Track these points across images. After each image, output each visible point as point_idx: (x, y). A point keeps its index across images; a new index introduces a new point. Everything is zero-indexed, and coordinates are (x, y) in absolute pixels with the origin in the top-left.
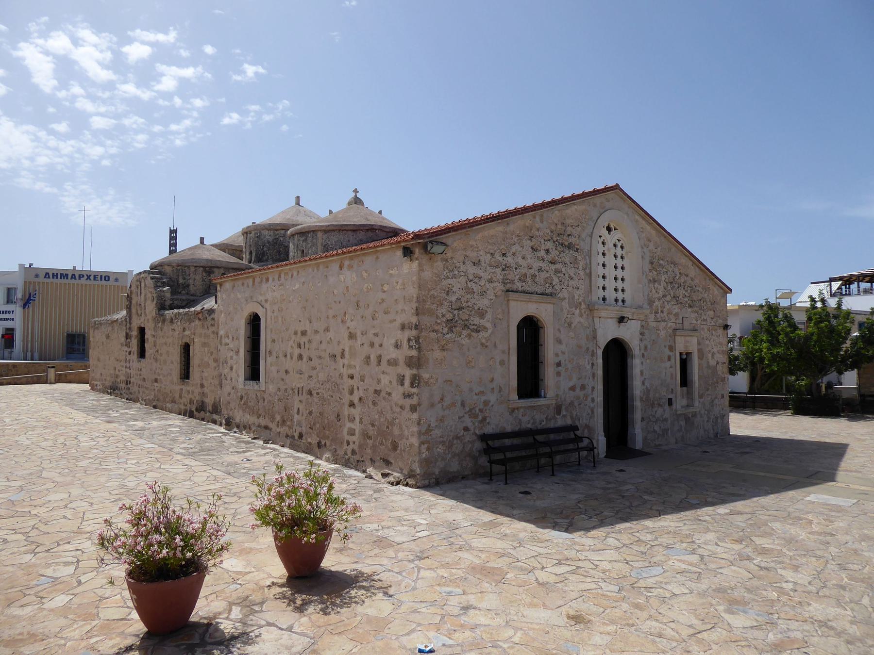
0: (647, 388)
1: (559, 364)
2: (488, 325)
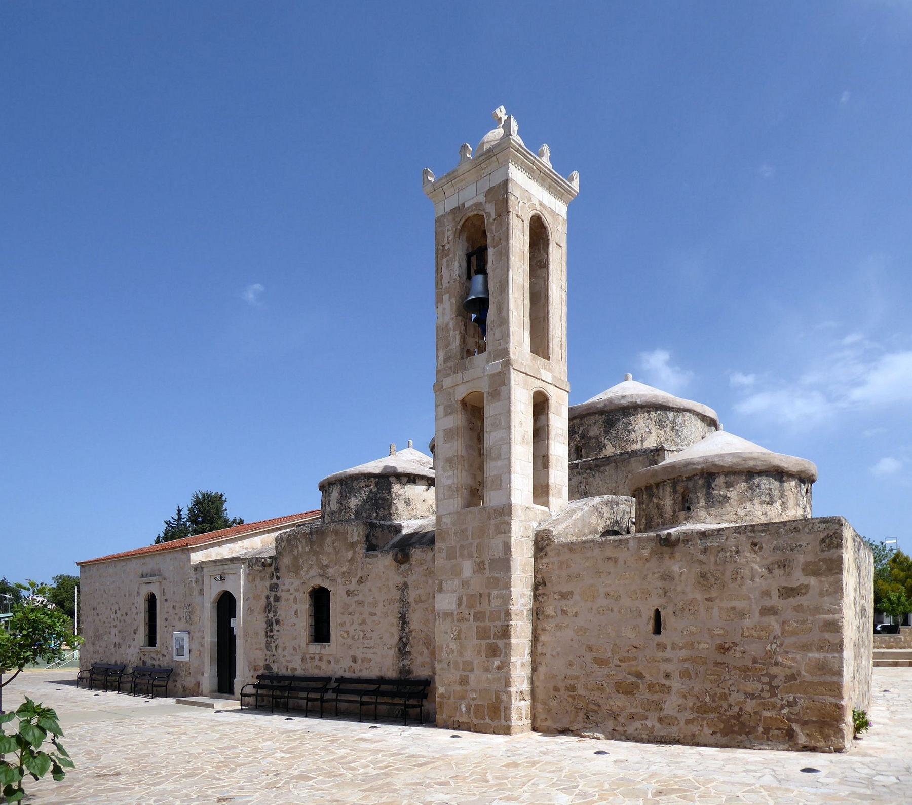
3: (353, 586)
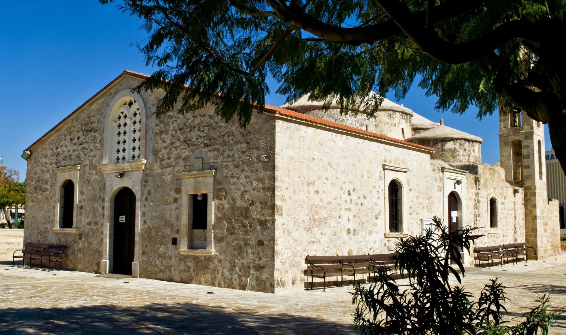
0: (149, 227)
1: (81, 208)
2: (49, 187)
3: (503, 200)
